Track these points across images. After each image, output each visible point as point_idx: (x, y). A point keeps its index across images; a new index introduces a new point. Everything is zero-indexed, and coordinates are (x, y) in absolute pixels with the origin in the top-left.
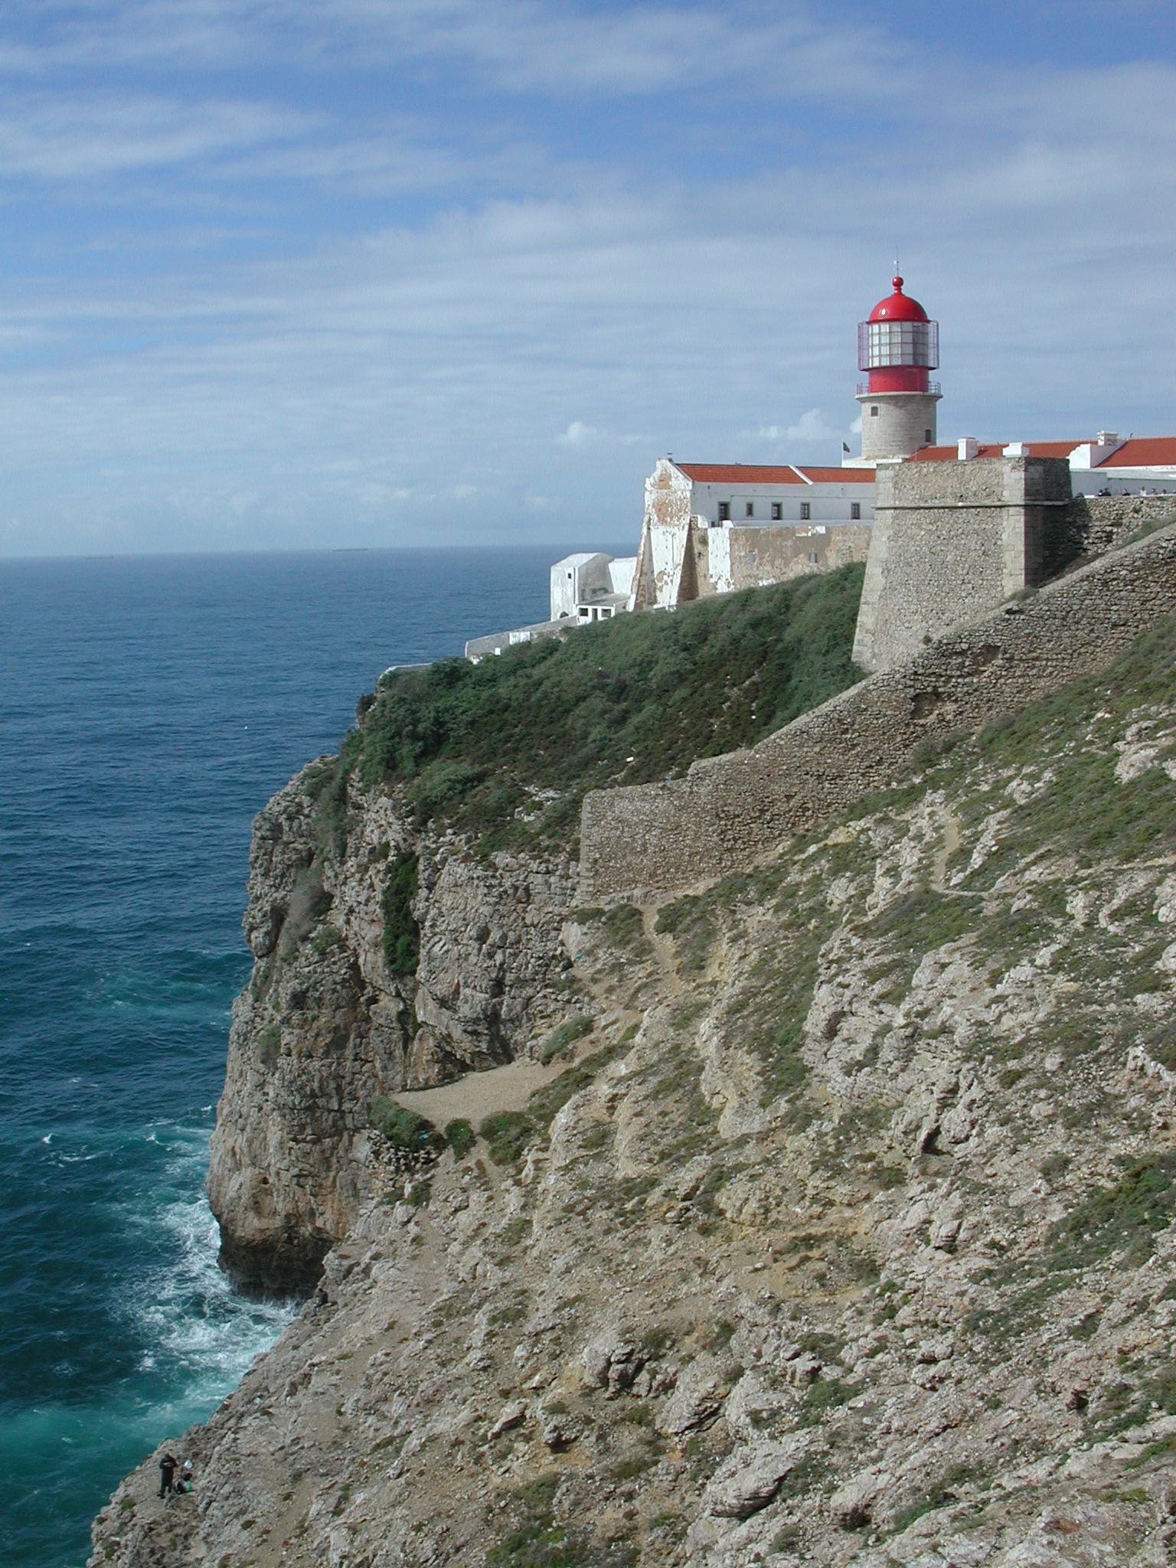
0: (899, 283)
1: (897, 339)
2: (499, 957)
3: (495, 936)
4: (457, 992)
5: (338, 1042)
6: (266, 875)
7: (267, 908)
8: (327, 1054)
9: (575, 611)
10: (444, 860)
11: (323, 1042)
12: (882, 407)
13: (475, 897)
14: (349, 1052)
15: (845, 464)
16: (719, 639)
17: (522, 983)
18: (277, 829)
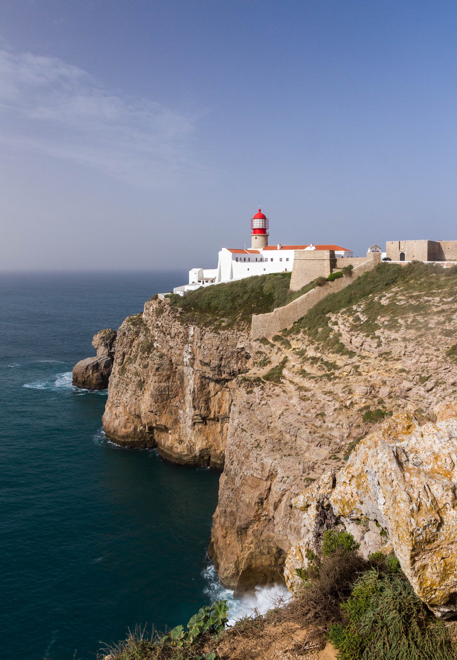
0: (260, 210)
1: (261, 223)
2: (222, 353)
3: (221, 348)
4: (211, 361)
5: (169, 378)
6: (121, 345)
7: (121, 353)
8: (165, 381)
9: (196, 281)
10: (205, 333)
11: (164, 378)
12: (257, 237)
13: (215, 341)
14: (171, 380)
15: (248, 249)
16: (250, 286)
17: (227, 358)
18: (124, 334)
